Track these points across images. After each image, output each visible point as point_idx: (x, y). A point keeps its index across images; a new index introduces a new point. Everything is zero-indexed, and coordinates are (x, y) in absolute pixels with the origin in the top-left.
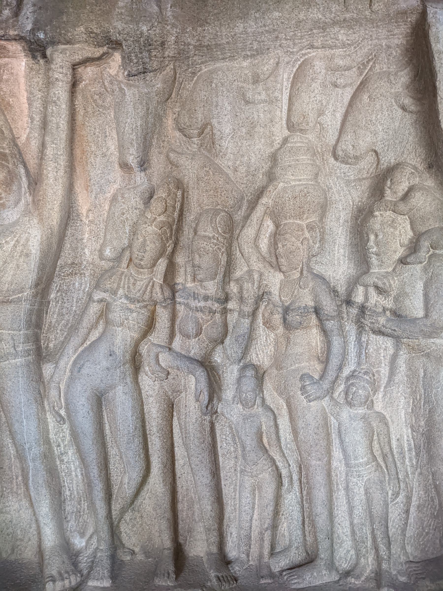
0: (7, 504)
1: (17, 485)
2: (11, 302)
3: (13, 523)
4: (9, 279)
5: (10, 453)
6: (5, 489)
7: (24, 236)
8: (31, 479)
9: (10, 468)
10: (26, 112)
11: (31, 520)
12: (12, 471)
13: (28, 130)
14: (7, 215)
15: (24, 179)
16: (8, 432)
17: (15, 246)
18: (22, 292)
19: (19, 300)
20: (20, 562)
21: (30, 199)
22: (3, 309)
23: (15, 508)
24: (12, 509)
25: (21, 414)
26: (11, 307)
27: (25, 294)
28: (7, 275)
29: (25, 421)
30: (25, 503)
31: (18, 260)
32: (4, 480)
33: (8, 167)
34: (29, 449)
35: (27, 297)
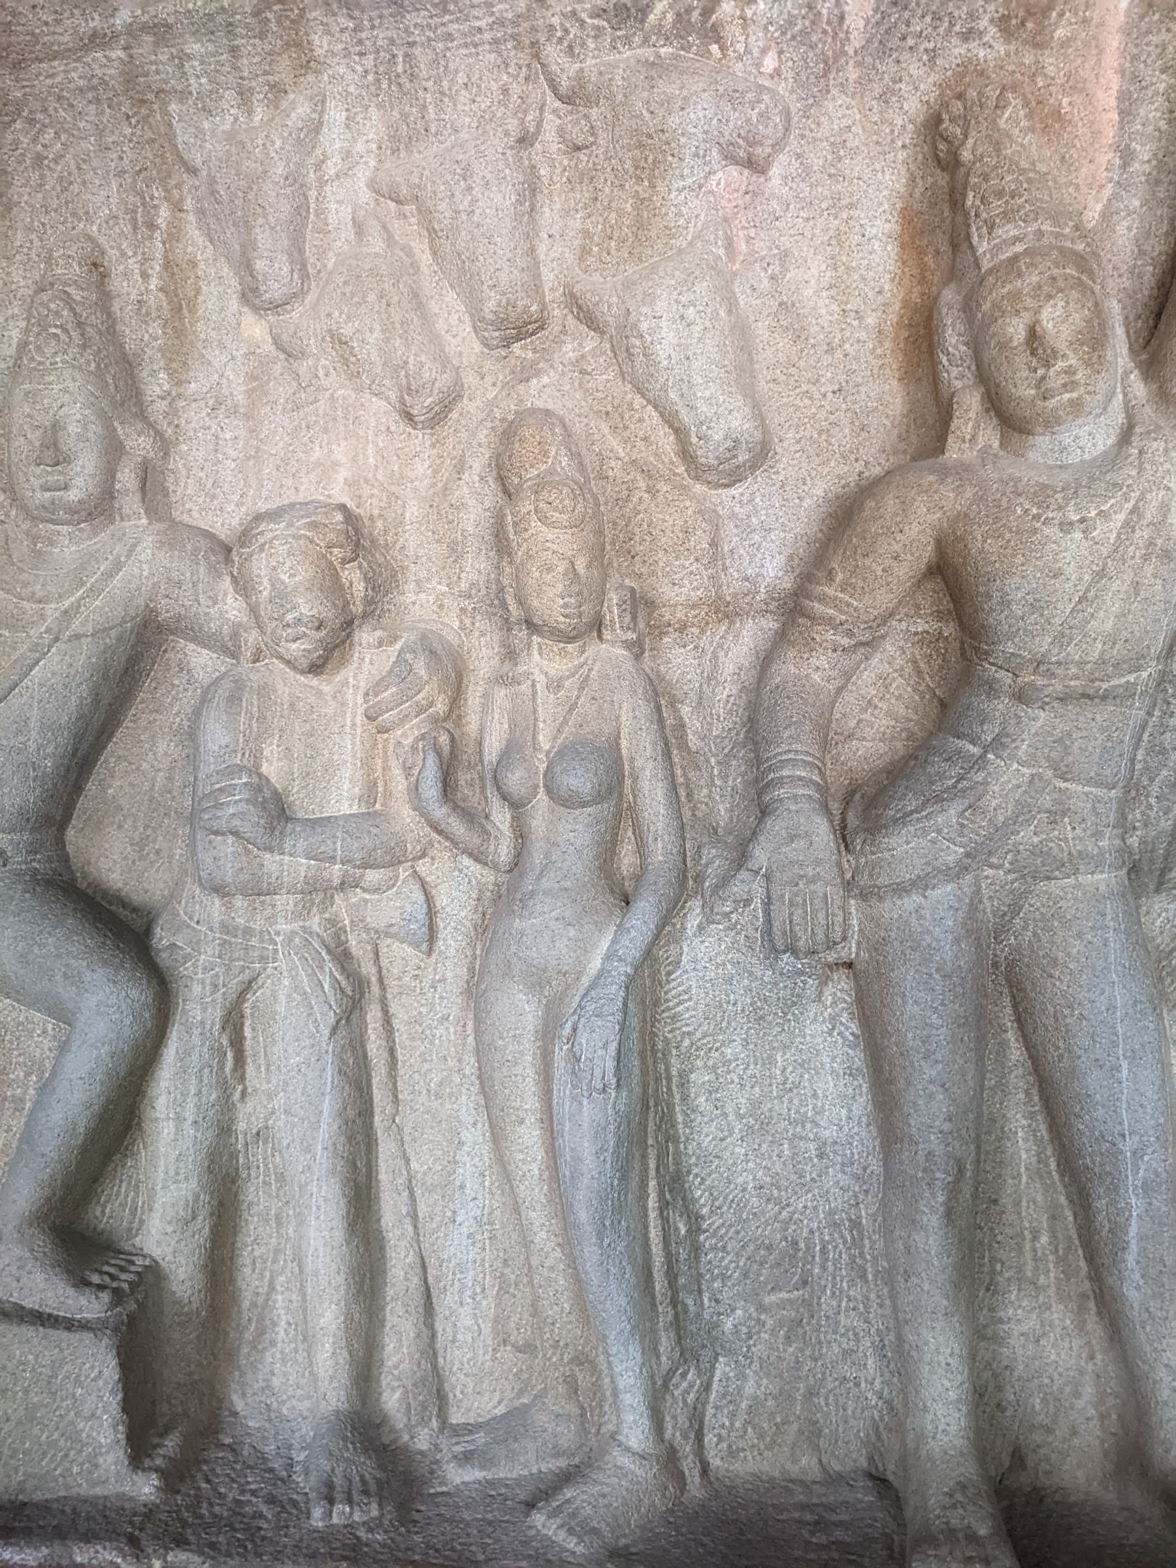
0: (1002, 1314)
1: (1035, 1259)
2: (1104, 698)
3: (1016, 1374)
4: (1109, 626)
5: (1020, 1157)
6: (998, 1267)
7: (1156, 498)
8: (1134, 1246)
9: (1017, 1204)
10: (1109, 135)
11: (1081, 1373)
12: (1020, 1214)
13: (1107, 192)
14: (1076, 437)
15: (1120, 331)
16: (1022, 1096)
17: (1129, 526)
18: (1138, 669)
19: (1129, 692)
20: (1057, 1497)
21: (1139, 389)
22: (1082, 719)
23: (1025, 1328)
24: (1017, 1329)
25: (1115, 1044)
26: (1103, 714)
27: (1145, 674)
28: (1101, 614)
29: (1125, 1065)
30: (1060, 1315)
31: (1138, 570)
32: (999, 1238)
33: (1093, 292)
34: (1134, 1153)
35: (1147, 685)
